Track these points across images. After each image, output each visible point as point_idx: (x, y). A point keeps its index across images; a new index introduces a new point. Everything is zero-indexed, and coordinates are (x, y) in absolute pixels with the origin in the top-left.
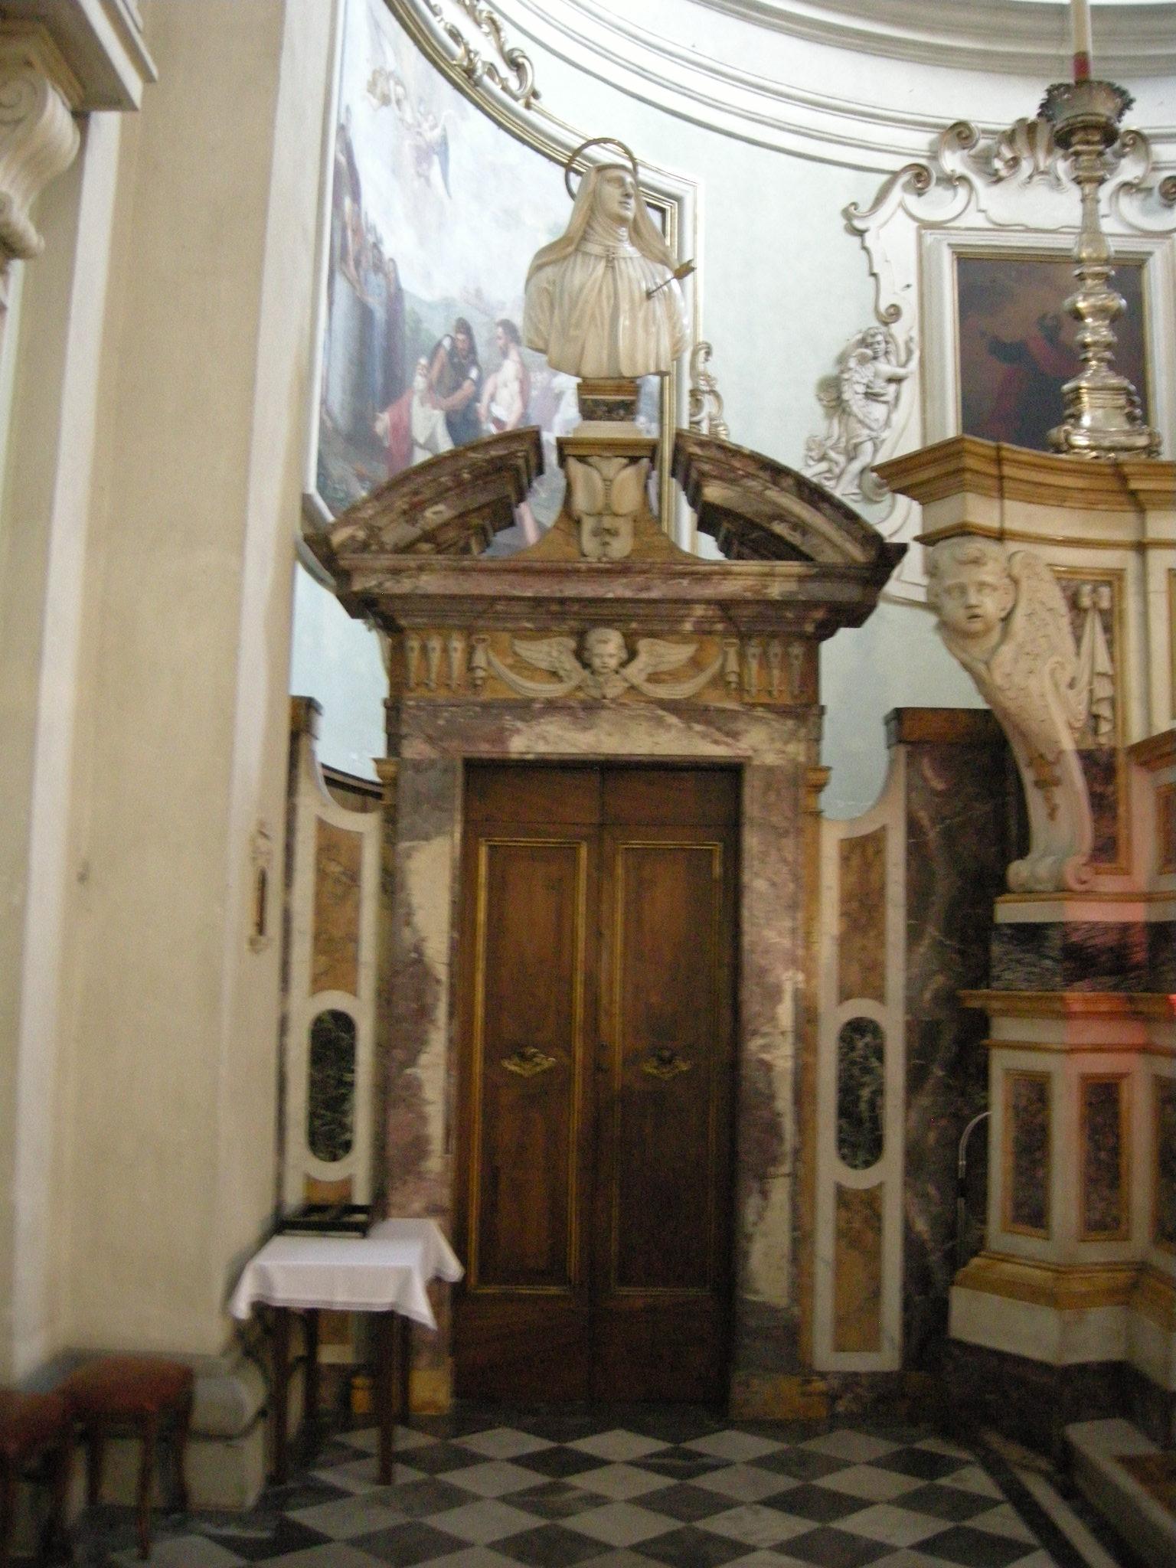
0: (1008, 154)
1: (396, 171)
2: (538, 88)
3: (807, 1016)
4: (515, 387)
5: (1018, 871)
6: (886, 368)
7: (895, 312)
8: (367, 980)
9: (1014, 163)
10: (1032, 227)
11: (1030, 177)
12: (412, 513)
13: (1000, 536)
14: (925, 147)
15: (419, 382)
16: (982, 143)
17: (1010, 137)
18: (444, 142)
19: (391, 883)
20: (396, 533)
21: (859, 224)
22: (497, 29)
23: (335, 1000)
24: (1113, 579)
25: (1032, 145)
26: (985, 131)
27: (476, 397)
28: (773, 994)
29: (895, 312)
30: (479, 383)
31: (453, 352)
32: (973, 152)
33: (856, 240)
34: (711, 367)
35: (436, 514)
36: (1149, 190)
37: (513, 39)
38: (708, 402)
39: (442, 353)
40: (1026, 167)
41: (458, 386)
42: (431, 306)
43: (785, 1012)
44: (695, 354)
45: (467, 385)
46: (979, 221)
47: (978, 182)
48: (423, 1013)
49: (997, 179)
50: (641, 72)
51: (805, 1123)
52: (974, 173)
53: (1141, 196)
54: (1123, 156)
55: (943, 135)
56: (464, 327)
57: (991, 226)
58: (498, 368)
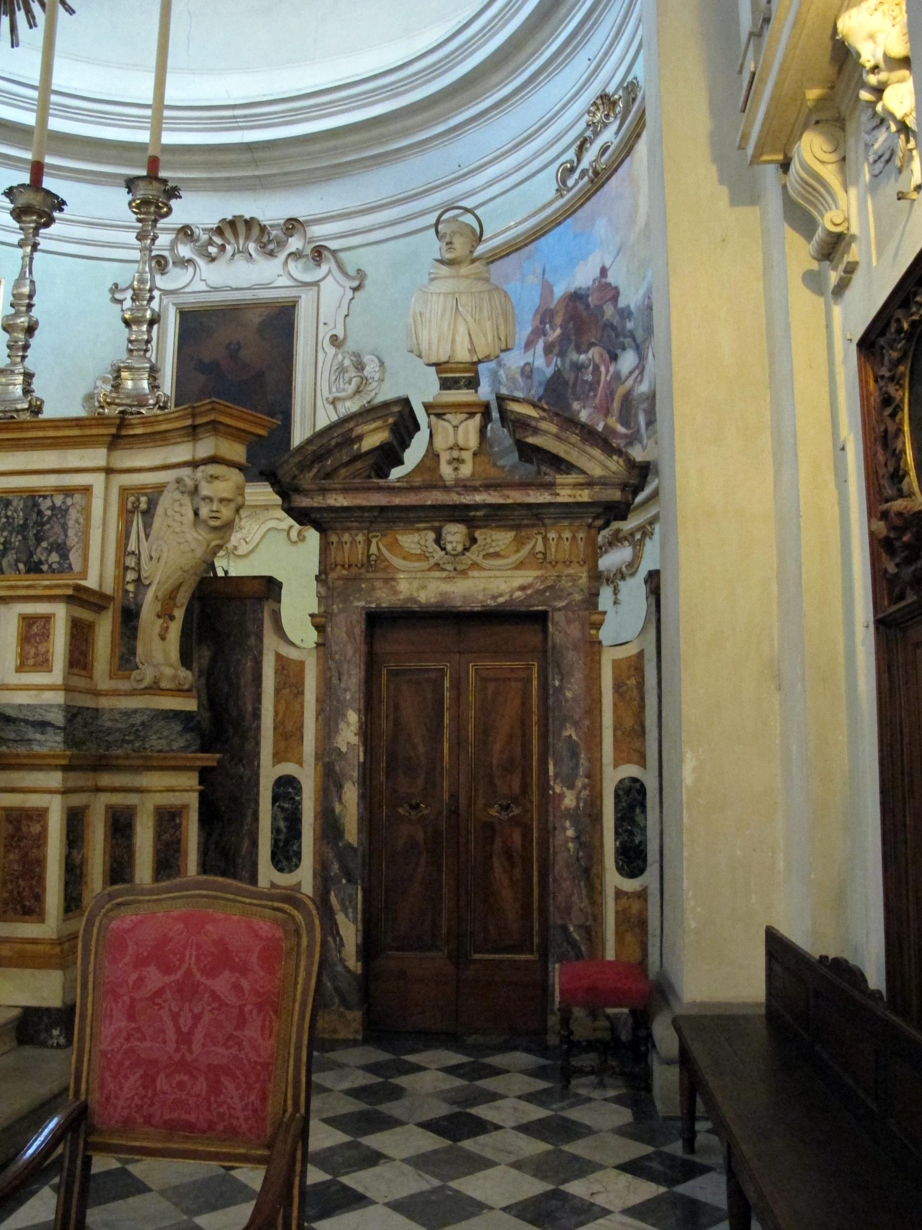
0: (218, 240)
9: (222, 248)
10: (234, 286)
11: (233, 255)
14: (168, 243)
16: (204, 237)
17: (219, 231)
21: (118, 296)
25: (236, 235)
26: (204, 230)
32: (198, 244)
33: (119, 306)
36: (307, 256)
46: (202, 287)
47: (201, 262)
52: (199, 257)
53: (304, 260)
54: (291, 236)
55: (177, 234)
57: (208, 289)
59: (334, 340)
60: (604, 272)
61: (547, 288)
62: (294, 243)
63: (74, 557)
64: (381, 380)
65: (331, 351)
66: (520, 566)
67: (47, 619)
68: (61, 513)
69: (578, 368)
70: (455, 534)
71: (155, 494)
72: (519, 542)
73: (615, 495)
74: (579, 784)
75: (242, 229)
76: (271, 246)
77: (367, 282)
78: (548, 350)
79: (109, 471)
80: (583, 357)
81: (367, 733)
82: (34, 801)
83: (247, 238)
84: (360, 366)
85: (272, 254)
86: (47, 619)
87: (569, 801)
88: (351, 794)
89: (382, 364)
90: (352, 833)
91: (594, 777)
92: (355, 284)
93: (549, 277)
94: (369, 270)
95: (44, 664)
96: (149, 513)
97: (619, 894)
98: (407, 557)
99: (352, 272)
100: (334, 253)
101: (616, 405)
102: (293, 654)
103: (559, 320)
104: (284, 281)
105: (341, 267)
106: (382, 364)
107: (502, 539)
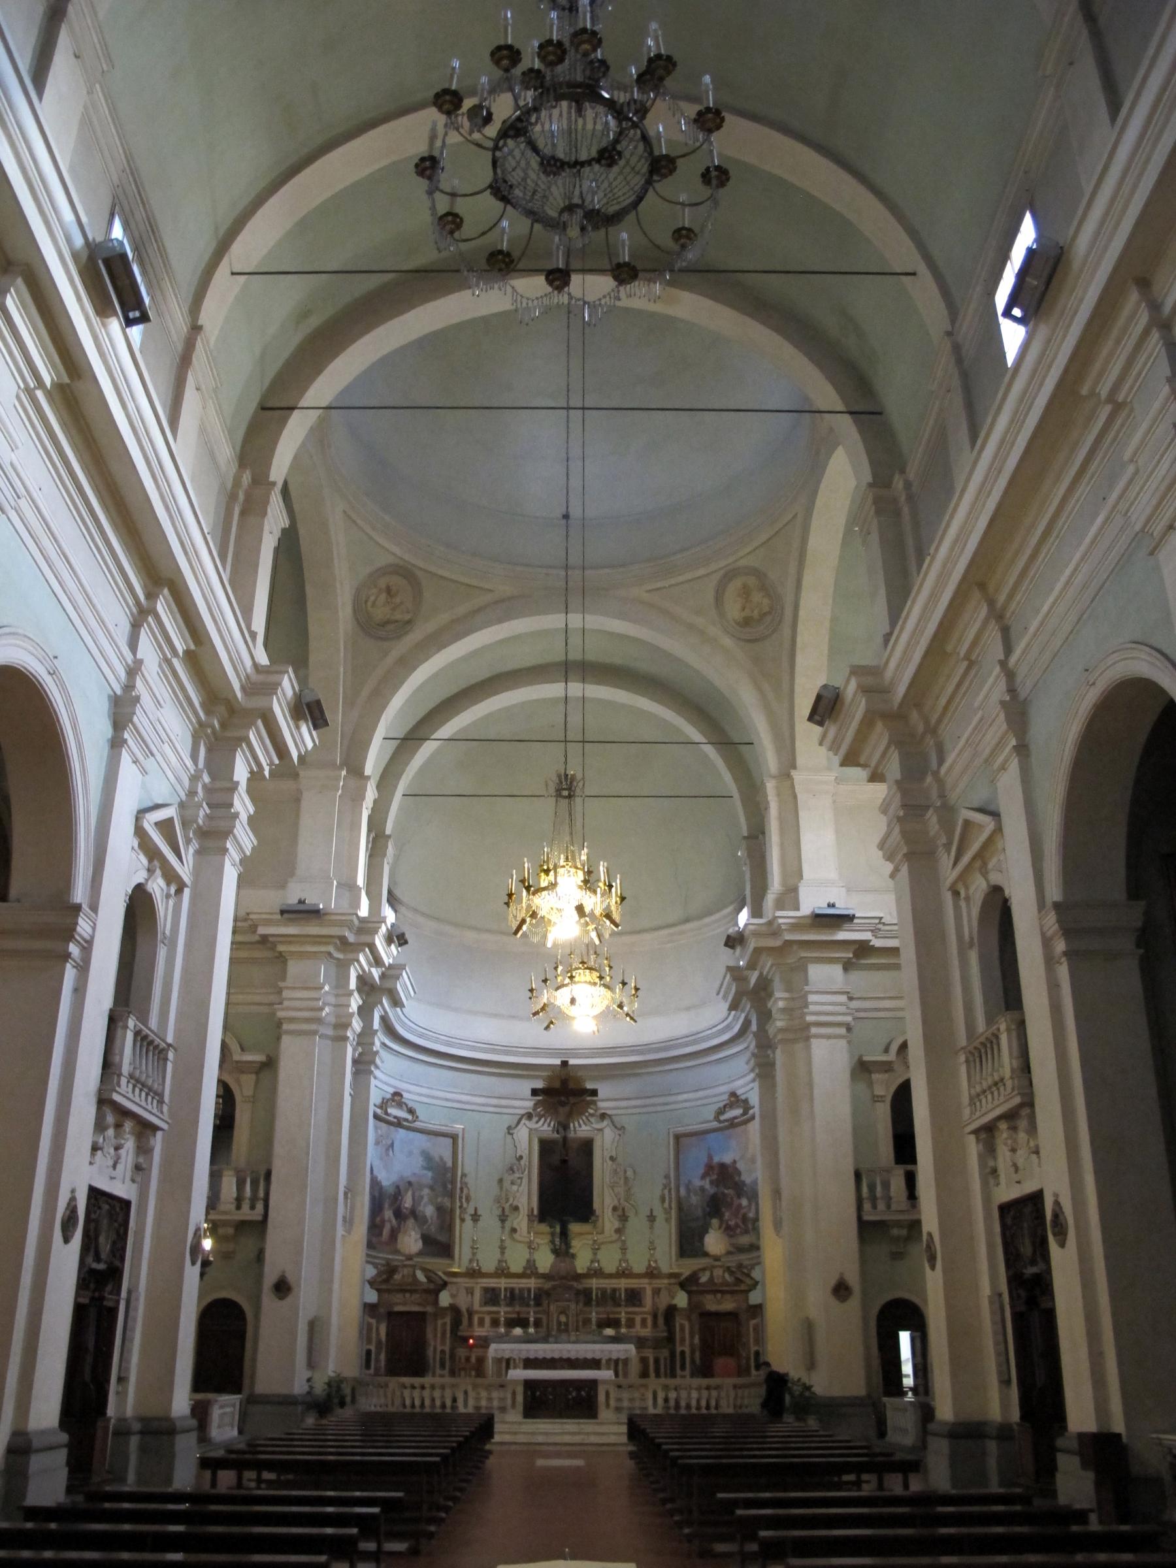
1: (381, 1159)
5: (461, 1328)
6: (517, 1175)
7: (521, 1157)
19: (377, 1329)
20: (380, 1279)
22: (407, 1106)
29: (521, 1157)
34: (466, 1180)
37: (410, 1104)
38: (465, 1191)
43: (432, 1349)
45: (398, 1202)
50: (447, 1100)
51: (435, 1366)
56: (398, 1187)
59: (612, 1158)
60: (735, 1162)
61: (710, 1158)
64: (634, 1179)
65: (610, 1163)
69: (723, 1194)
70: (719, 1295)
78: (712, 1183)
80: (726, 1191)
81: (701, 1339)
82: (648, 1355)
87: (744, 1355)
88: (697, 1354)
89: (634, 1172)
90: (698, 1361)
99: (619, 1126)
100: (610, 1116)
101: (740, 1216)
102: (683, 1322)
105: (613, 1122)
107: (728, 1296)
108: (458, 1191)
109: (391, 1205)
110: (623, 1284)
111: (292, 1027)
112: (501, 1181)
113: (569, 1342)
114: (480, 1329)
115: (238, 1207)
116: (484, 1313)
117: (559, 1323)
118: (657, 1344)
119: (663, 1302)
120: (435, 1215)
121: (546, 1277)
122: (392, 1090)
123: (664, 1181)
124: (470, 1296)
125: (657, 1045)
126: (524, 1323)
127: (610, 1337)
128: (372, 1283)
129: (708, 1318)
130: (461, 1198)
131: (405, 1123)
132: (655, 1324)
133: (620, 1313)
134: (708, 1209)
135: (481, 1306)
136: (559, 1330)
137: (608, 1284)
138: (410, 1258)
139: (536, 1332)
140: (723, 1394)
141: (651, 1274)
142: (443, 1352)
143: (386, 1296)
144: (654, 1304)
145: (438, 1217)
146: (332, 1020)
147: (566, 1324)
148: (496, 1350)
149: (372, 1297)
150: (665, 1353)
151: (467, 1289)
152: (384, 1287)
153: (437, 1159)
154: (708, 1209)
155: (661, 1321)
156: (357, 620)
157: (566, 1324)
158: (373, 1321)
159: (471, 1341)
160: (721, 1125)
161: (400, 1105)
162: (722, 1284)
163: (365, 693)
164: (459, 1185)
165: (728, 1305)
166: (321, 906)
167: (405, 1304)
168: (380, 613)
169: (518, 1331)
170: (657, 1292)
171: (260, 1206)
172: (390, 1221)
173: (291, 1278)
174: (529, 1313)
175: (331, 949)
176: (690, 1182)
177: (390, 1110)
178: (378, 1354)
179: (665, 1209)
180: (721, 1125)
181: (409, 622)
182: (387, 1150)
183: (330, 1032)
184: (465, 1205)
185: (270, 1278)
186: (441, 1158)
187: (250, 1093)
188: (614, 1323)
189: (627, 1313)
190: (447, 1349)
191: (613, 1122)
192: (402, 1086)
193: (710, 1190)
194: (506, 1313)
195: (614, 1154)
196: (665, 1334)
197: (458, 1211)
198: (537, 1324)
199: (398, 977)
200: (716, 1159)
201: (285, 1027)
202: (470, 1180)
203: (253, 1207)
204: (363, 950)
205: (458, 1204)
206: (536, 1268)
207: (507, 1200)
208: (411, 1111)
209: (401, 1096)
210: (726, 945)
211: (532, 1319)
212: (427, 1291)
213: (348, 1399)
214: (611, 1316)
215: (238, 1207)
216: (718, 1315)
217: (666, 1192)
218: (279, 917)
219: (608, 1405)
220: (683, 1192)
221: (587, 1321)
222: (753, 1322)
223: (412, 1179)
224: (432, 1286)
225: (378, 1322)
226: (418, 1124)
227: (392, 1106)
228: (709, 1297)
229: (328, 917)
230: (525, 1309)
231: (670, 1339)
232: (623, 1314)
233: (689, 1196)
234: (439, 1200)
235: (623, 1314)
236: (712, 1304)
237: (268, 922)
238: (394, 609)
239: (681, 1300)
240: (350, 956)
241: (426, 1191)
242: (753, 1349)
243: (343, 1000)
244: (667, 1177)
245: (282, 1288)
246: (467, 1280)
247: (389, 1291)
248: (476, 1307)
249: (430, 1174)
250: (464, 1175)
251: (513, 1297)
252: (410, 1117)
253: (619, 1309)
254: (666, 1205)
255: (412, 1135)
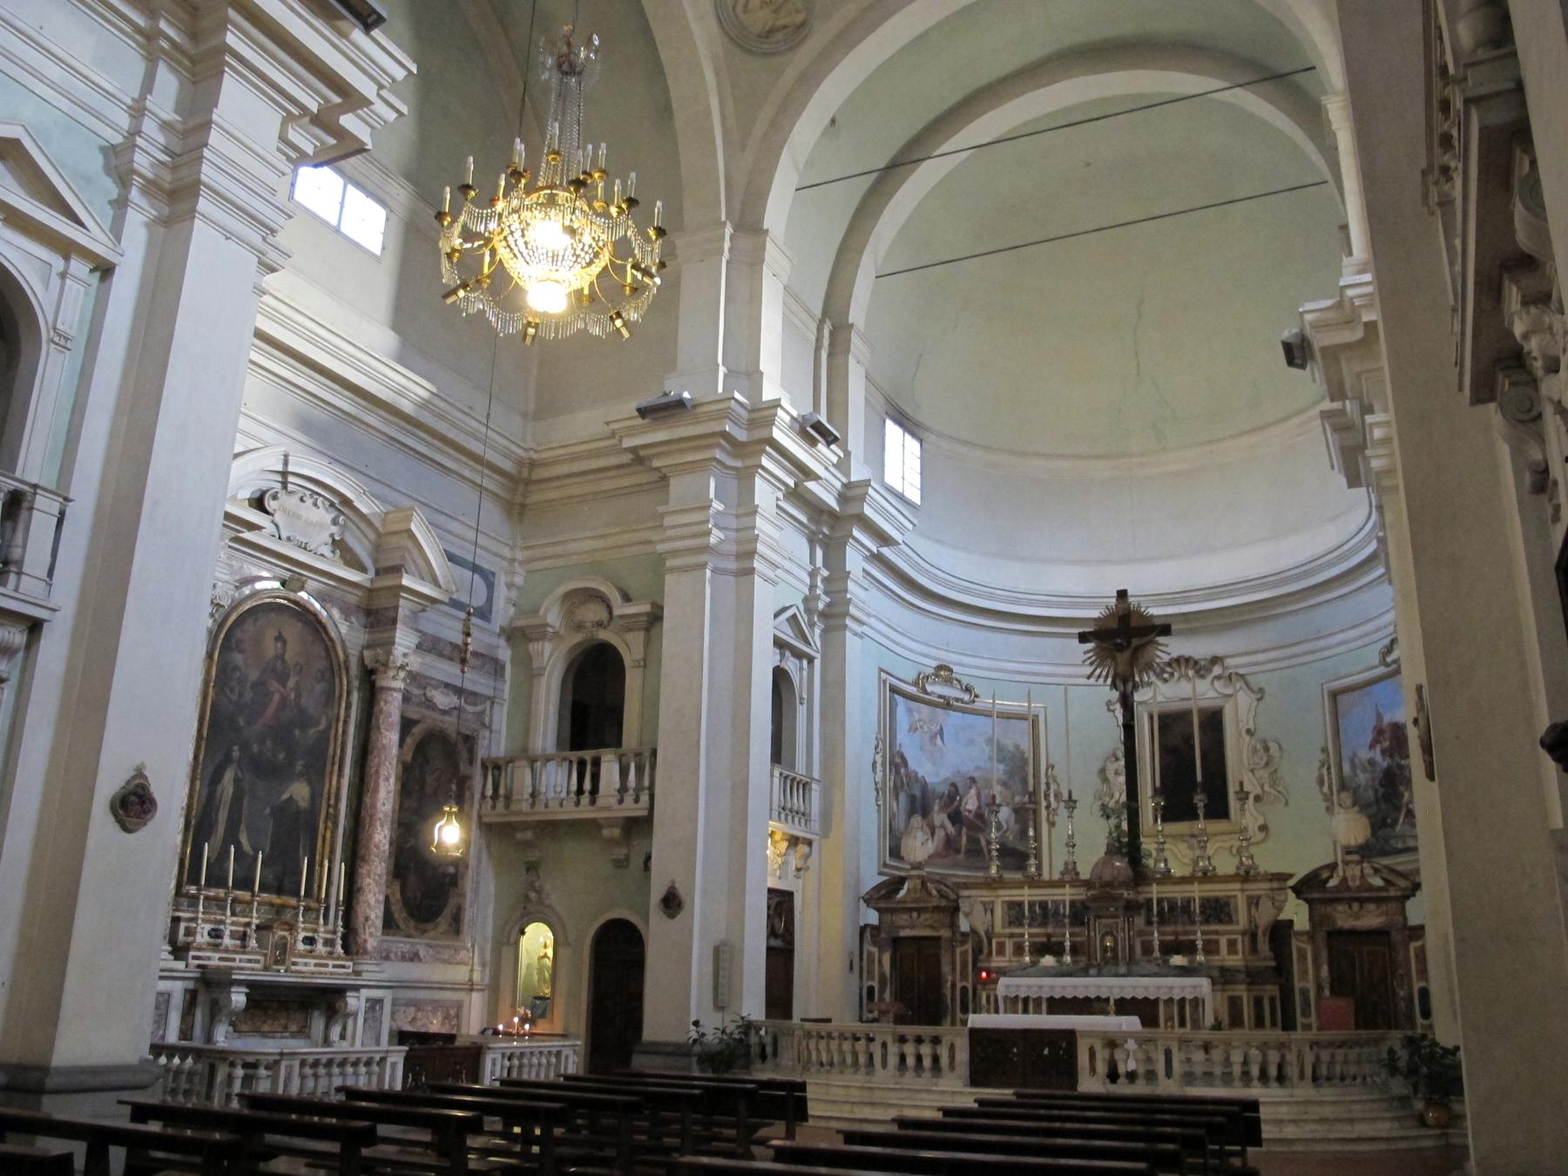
0: (1169, 669)
1: (922, 749)
2: (977, 692)
3: (953, 986)
4: (975, 798)
5: (982, 957)
8: (877, 979)
9: (1172, 674)
12: (879, 891)
13: (969, 897)
15: (936, 808)
18: (941, 729)
20: (876, 896)
21: (1112, 708)
22: (959, 682)
23: (870, 983)
24: (993, 903)
25: (1179, 665)
27: (960, 805)
28: (947, 981)
30: (961, 800)
31: (949, 795)
33: (1111, 714)
34: (1056, 772)
35: (883, 892)
37: (965, 681)
38: (1053, 787)
39: (945, 797)
40: (1176, 675)
41: (952, 803)
42: (939, 783)
43: (949, 984)
44: (1047, 770)
45: (956, 803)
47: (1159, 683)
48: (886, 984)
49: (1166, 681)
50: (1020, 673)
56: (954, 785)
58: (968, 792)
59: (1248, 731)
61: (1379, 716)
62: (1217, 670)
63: (1234, 918)
64: (1281, 757)
65: (1247, 738)
66: (1378, 916)
67: (1236, 940)
68: (1227, 904)
71: (1258, 898)
72: (1378, 908)
73: (1408, 893)
74: (1405, 987)
75: (1183, 663)
76: (1202, 672)
77: (1266, 696)
78: (1383, 752)
79: (1242, 890)
81: (1331, 971)
83: (1186, 667)
84: (1267, 749)
85: (1203, 677)
86: (1236, 940)
87: (1402, 993)
89: (1280, 747)
91: (1411, 988)
92: (1259, 696)
93: (1381, 710)
94: (1267, 688)
95: (1236, 952)
96: (1257, 905)
97: (1422, 1025)
98: (1341, 913)
99: (1255, 689)
100: (1242, 676)
102: (1302, 945)
103: (1388, 735)
104: (1212, 694)
105: (1247, 684)
106: (1280, 747)
107: (1371, 907)
108: (1043, 787)
109: (944, 807)
110: (1197, 891)
111: (677, 562)
112: (1103, 771)
113: (1117, 975)
114: (1000, 958)
115: (621, 801)
116: (1003, 935)
117: (1105, 949)
118: (1253, 977)
119: (1265, 916)
120: (1013, 818)
121: (1087, 884)
122: (935, 664)
123: (1322, 757)
124: (989, 913)
125: (1296, 571)
126: (1056, 949)
127: (1181, 967)
128: (869, 900)
129: (1338, 942)
130: (1047, 796)
131: (955, 703)
132: (1254, 949)
133: (1195, 933)
134: (1381, 790)
135: (1003, 927)
136: (1103, 957)
137: (1177, 892)
138: (918, 866)
139: (1074, 962)
140: (1291, 1057)
141: (1246, 876)
142: (964, 989)
143: (888, 917)
144: (1251, 919)
145: (1017, 821)
146: (732, 548)
147: (1114, 950)
148: (1007, 987)
149: (872, 917)
150: (1272, 990)
151: (984, 904)
152: (882, 905)
153: (1011, 748)
154: (1381, 790)
155: (1264, 946)
156: (728, 35)
157: (1114, 950)
158: (875, 950)
159: (984, 974)
160: (1390, 669)
161: (948, 681)
162: (1359, 889)
163: (758, 131)
164: (1043, 780)
165: (1371, 919)
166: (686, 395)
167: (913, 927)
168: (760, 19)
169: (1048, 960)
170: (1254, 902)
171: (645, 798)
172: (942, 826)
173: (682, 891)
174: (1064, 935)
175: (718, 454)
176: (1355, 754)
177: (929, 688)
178: (882, 991)
179: (1325, 795)
180: (1390, 669)
181: (803, 24)
182: (933, 737)
183: (732, 565)
184: (1054, 805)
185: (657, 893)
186: (1017, 747)
187: (640, 656)
188: (1188, 948)
189: (1203, 933)
190: (970, 987)
191: (1247, 684)
192: (947, 658)
193: (1384, 763)
194: (1030, 935)
195: (1251, 725)
196: (1273, 964)
197: (1044, 813)
198: (1075, 950)
199: (862, 498)
200: (1388, 719)
201: (669, 563)
202: (1059, 772)
203: (637, 800)
204: (764, 451)
205: (1044, 804)
206: (1077, 874)
207: (1112, 796)
208: (968, 690)
209: (951, 670)
210: (1291, 362)
211: (1068, 944)
212: (937, 909)
213: (769, 1050)
214: (1182, 938)
215: (621, 801)
216: (1353, 933)
217: (1325, 771)
218: (640, 421)
219: (1093, 1070)
220: (1346, 768)
221: (1147, 949)
222: (1414, 945)
223: (976, 775)
224: (944, 903)
225: (879, 952)
226: (978, 705)
227: (934, 682)
228: (1341, 908)
229: (699, 410)
230: (1058, 930)
231: (1282, 970)
232: (1199, 934)
233: (1356, 775)
234: (1017, 799)
235: (1199, 934)
236: (1344, 918)
237: (632, 432)
238: (777, 11)
239: (1297, 913)
240: (749, 462)
241: (997, 790)
242: (1417, 985)
243: (745, 521)
244: (1324, 750)
245: (672, 903)
246: (984, 892)
247: (893, 911)
248: (998, 928)
249: (1002, 767)
250: (1050, 767)
251: (1045, 913)
252: (966, 697)
253: (1193, 928)
254: (1326, 789)
255: (970, 718)
